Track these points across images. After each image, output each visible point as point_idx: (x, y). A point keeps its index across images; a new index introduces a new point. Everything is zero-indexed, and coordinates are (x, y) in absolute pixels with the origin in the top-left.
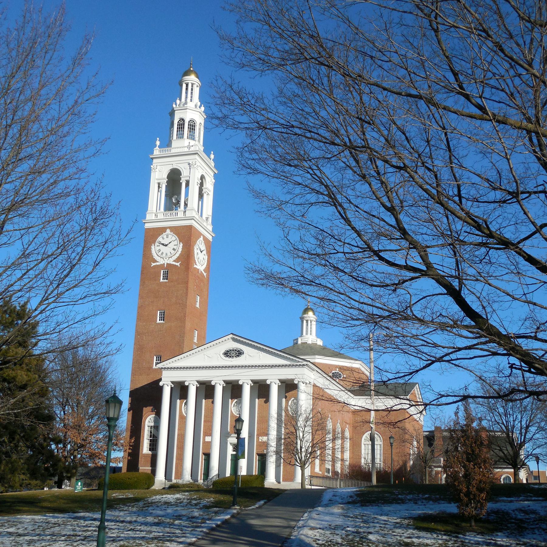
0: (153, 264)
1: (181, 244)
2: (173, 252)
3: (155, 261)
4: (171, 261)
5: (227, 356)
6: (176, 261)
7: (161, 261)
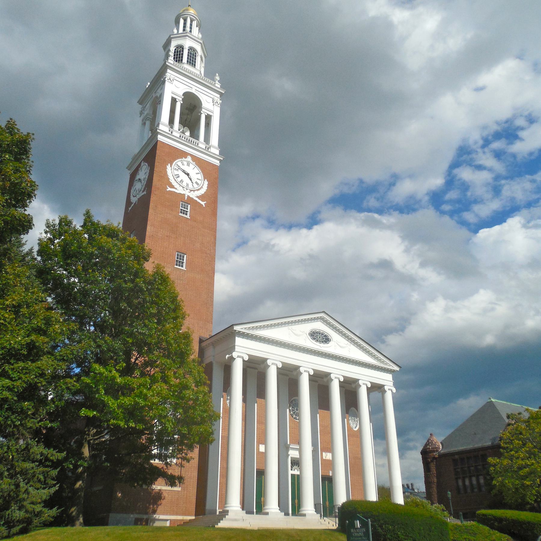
0: (169, 189)
1: (206, 183)
2: (195, 186)
3: (172, 187)
4: (194, 195)
5: (314, 339)
6: (201, 197)
7: (180, 190)
